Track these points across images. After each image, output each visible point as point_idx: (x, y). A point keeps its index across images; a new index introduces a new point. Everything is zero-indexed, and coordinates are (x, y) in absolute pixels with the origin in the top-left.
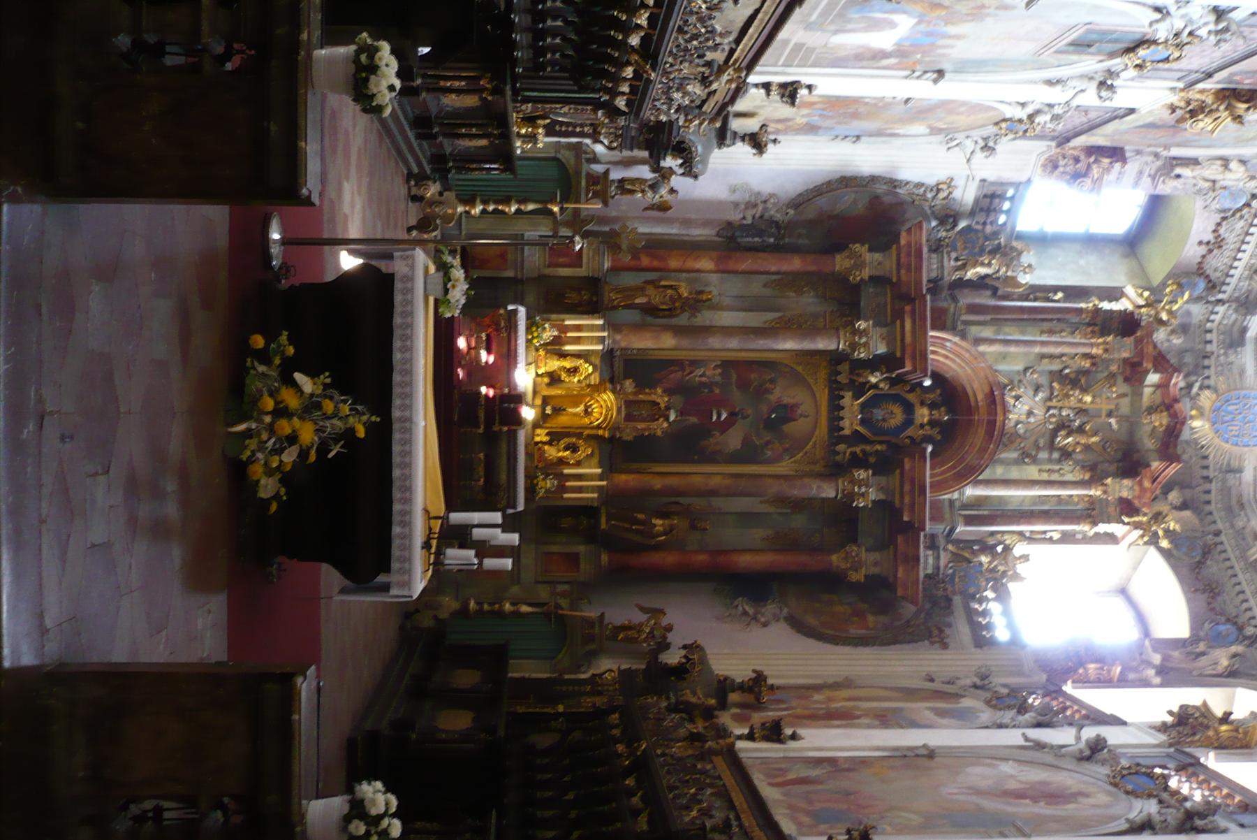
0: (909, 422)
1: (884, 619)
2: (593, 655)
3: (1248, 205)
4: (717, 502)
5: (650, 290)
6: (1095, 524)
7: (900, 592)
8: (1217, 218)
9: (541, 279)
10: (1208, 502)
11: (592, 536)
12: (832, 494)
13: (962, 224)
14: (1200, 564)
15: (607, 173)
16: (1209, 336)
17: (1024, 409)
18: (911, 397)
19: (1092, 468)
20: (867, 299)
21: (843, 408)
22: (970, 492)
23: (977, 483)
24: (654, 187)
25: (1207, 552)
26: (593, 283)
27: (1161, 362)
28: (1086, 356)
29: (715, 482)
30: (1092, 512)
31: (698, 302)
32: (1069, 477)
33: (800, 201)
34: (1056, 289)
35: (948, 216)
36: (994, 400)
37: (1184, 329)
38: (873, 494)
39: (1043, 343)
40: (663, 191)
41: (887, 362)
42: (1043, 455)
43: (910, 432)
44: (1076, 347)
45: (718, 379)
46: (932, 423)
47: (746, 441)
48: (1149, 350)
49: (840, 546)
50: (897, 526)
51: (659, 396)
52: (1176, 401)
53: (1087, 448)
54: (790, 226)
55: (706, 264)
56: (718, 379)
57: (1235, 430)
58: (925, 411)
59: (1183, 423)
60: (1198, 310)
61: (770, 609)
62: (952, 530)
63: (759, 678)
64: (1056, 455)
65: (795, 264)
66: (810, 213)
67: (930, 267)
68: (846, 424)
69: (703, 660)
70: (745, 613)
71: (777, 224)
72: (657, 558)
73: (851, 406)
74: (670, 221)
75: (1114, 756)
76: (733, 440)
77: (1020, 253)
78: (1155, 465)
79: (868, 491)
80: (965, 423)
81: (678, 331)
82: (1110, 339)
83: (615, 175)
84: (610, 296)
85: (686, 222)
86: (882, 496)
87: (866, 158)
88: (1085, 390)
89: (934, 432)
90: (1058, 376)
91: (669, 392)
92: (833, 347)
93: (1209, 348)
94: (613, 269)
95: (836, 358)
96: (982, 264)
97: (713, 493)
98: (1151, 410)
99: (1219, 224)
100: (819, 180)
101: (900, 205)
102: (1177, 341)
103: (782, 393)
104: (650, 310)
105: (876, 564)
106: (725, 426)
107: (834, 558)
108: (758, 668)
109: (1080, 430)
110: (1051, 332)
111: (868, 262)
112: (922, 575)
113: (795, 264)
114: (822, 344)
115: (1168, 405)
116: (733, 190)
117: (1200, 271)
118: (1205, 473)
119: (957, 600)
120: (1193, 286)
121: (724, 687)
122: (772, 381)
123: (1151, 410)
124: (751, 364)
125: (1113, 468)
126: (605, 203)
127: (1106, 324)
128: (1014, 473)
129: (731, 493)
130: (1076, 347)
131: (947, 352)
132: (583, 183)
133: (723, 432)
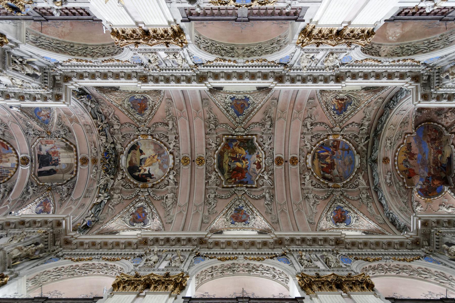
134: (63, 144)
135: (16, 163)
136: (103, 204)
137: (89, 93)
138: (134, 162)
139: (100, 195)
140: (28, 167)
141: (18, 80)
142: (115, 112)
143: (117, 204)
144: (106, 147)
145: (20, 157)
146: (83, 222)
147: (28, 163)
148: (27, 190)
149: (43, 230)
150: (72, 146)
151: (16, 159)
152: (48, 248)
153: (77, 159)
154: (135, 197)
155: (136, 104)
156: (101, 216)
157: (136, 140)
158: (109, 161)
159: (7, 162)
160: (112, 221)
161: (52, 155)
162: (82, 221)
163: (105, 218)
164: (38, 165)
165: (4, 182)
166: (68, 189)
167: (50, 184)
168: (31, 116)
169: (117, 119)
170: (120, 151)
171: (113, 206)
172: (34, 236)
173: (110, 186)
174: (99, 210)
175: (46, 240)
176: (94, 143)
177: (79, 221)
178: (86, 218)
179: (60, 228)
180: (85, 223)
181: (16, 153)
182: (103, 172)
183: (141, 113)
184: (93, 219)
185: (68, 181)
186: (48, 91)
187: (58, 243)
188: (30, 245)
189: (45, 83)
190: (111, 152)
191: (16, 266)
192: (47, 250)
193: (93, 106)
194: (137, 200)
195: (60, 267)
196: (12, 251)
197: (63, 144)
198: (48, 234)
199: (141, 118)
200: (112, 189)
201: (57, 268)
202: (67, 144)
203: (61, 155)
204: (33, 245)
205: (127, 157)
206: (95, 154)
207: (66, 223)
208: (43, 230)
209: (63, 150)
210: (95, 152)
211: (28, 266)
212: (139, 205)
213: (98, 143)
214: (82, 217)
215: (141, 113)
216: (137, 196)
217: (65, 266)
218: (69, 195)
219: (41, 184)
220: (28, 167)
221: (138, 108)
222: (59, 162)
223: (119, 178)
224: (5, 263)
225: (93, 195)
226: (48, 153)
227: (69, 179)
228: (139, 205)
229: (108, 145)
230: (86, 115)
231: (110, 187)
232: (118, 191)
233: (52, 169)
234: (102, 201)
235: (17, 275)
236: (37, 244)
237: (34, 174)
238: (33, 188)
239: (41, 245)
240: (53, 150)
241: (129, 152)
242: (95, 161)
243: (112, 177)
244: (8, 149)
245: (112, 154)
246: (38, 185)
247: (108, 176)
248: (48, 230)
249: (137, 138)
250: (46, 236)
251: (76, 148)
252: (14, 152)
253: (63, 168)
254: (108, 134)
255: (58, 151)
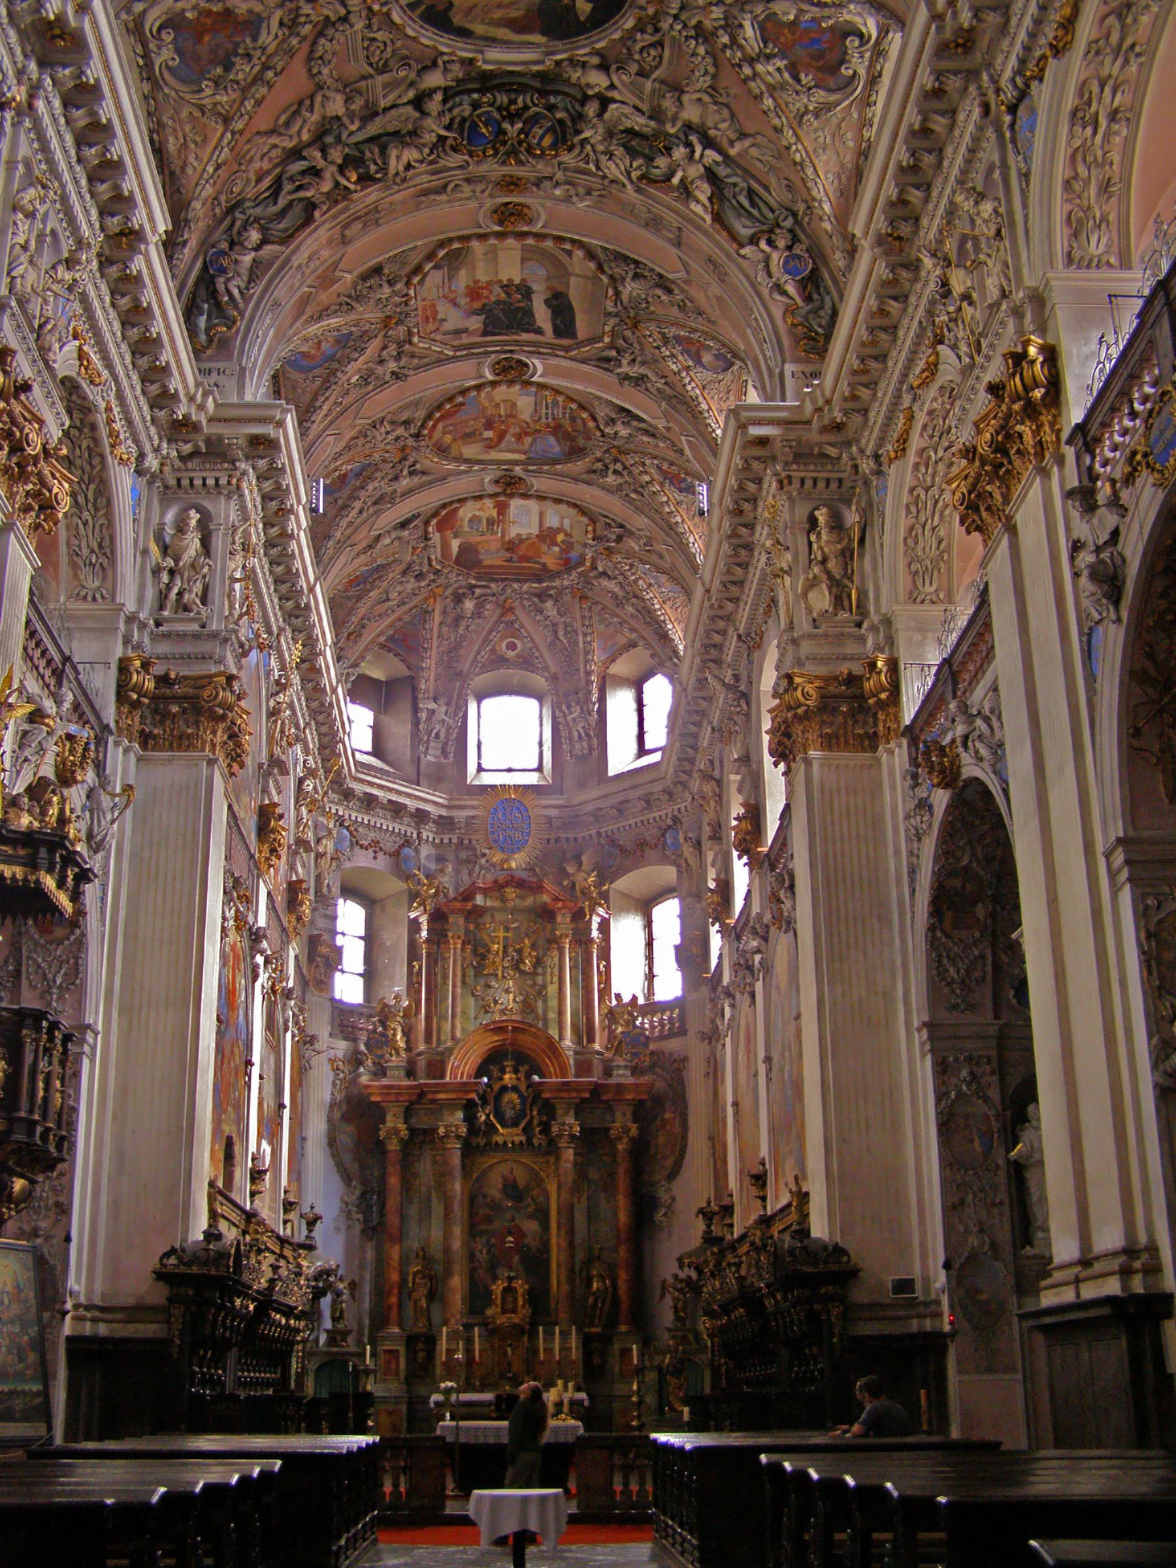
0: (515, 1089)
1: (668, 1104)
2: (697, 1334)
3: (347, 828)
4: (578, 1240)
5: (415, 1295)
6: (592, 940)
7: (645, 1097)
8: (357, 849)
9: (408, 1381)
10: (576, 839)
11: (606, 1339)
12: (571, 1152)
13: (362, 1047)
14: (622, 850)
15: (327, 1331)
16: (446, 841)
17: (507, 998)
18: (496, 1087)
19: (550, 942)
20: (422, 1121)
21: (505, 1142)
22: (568, 1042)
23: (561, 1037)
24: (338, 1294)
25: (613, 842)
26: (411, 1341)
27: (468, 896)
28: (463, 949)
29: (564, 1245)
30: (582, 940)
31: (425, 1257)
32: (556, 960)
33: (346, 1177)
34: (410, 967)
35: (356, 1060)
36: (499, 1029)
37: (440, 859)
38: (570, 1120)
39: (454, 986)
40: (341, 1286)
41: (470, 1109)
42: (539, 980)
43: (523, 1087)
44: (454, 956)
45: (484, 1239)
46: (516, 1071)
47: (531, 1217)
48: (457, 905)
49: (612, 1143)
50: (595, 1100)
51: (498, 1288)
52: (496, 881)
53: (534, 947)
54: (364, 1182)
55: (395, 1253)
56: (484, 1239)
57: (517, 835)
58: (507, 1076)
59: (513, 877)
60: (425, 851)
61: (663, 1195)
62: (598, 1053)
63: (701, 1211)
64: (540, 970)
65: (394, 1181)
66: (354, 1167)
67: (396, 1078)
68: (517, 1139)
69: (689, 1255)
70: (665, 1214)
71: (363, 1194)
72: (623, 1286)
73: (503, 1133)
74: (362, 1278)
75: (732, 983)
76: (531, 1227)
77: (386, 1005)
78: (546, 898)
79: (570, 1123)
80: (515, 1050)
81: (448, 1273)
82: (450, 934)
83: (328, 1324)
84: (421, 1327)
85: (362, 1267)
86: (572, 1112)
87: (317, 1127)
88: (489, 951)
89: (523, 1069)
90: (479, 971)
91: (495, 1279)
92: (459, 1153)
93: (455, 841)
94: (400, 1324)
95: (469, 1150)
96: (395, 1035)
97: (571, 1245)
98: (503, 899)
99: (361, 846)
100: (331, 1163)
101: (349, 1099)
102: (450, 868)
103: (494, 1188)
104: (432, 1296)
105: (624, 1114)
106: (519, 1233)
107: (620, 1147)
108: (695, 1211)
109: (520, 952)
110: (445, 977)
111: (394, 1122)
112: (631, 1080)
113: (394, 1181)
114: (456, 1160)
115: (498, 887)
116: (337, 1230)
117: (396, 854)
118: (552, 842)
119: (652, 1046)
120: (407, 858)
121: (709, 1239)
122: (485, 1197)
123: (503, 899)
124: (472, 1215)
125: (549, 926)
126: (350, 1332)
127: (438, 937)
128: (553, 1003)
129: (571, 1232)
130: (454, 956)
131: (461, 1067)
132: (335, 1349)
133: (525, 1235)
134: (435, 278)
135: (518, 387)
136: (722, 171)
137: (199, 264)
138: (514, 14)
139: (675, 181)
140: (536, 362)
141: (232, 565)
142: (263, 128)
143: (733, 115)
144: (442, 139)
145: (490, 377)
146: (784, 293)
147: (520, 361)
148: (626, 377)
149: (770, 485)
150: (441, 253)
151: (503, 388)
152: (840, 481)
153: (500, 236)
154: (706, 40)
155: (203, 50)
156: (776, 195)
157: (396, 17)
158: (512, 118)
159: (514, 405)
160: (810, 172)
161: (484, 301)
162: (778, 297)
163: (789, 188)
164: (526, 336)
165: (594, 419)
166: (636, 276)
167: (612, 321)
168: (326, 381)
169: (297, 112)
170: (457, 71)
171: (743, 135)
172: (786, 516)
173: (639, 122)
174: (751, 194)
175: (809, 484)
176: (426, 193)
177: (777, 313)
178: (770, 276)
179: (778, 444)
180: (791, 289)
181: (478, 387)
182: (567, 158)
183: (247, 22)
184: (781, 243)
185: (600, 268)
186: (244, 473)
187: (832, 452)
188: (810, 544)
189: (217, 484)
190: (467, 110)
191: (863, 594)
192: (847, 484)
193: (254, 236)
194: (725, 39)
195: (905, 498)
196: (809, 610)
197: (435, 278)
198: (789, 477)
199: (275, 22)
200: (656, 114)
201: (908, 507)
202: (435, 267)
203: (483, 275)
204: (813, 538)
205: (492, 41)
206: (479, 188)
207: (759, 422)
208: (770, 485)
209: (463, 272)
210: (467, 189)
211: (875, 569)
212: (749, 32)
213: (423, 178)
214: (765, 292)
215: (253, 24)
216: (702, 34)
217: (909, 481)
218: (664, 284)
219: (607, 340)
220: (538, 363)
221: (221, 38)
222: (517, 281)
223: (598, 80)
224: (842, 634)
225: (672, 219)
226: (475, 313)
227: (592, 265)
228: (749, 32)
229: (433, 128)
230: (300, 258)
231: (642, 120)
232: (668, 103)
233: (547, 302)
234: (711, 175)
235: (887, 622)
236: (813, 522)
237: (567, 349)
238: (625, 362)
239: (821, 516)
240: (463, 301)
241: (464, 33)
242: (511, 184)
243: (591, 109)
244: (463, 404)
245: (475, 105)
246: (612, 346)
247: (586, 134)
248: (776, 474)
249: (388, 14)
250: (796, 484)
251: (450, 240)
252: (474, 393)
253: (542, 272)
254: (373, 129)
255: (468, 287)
